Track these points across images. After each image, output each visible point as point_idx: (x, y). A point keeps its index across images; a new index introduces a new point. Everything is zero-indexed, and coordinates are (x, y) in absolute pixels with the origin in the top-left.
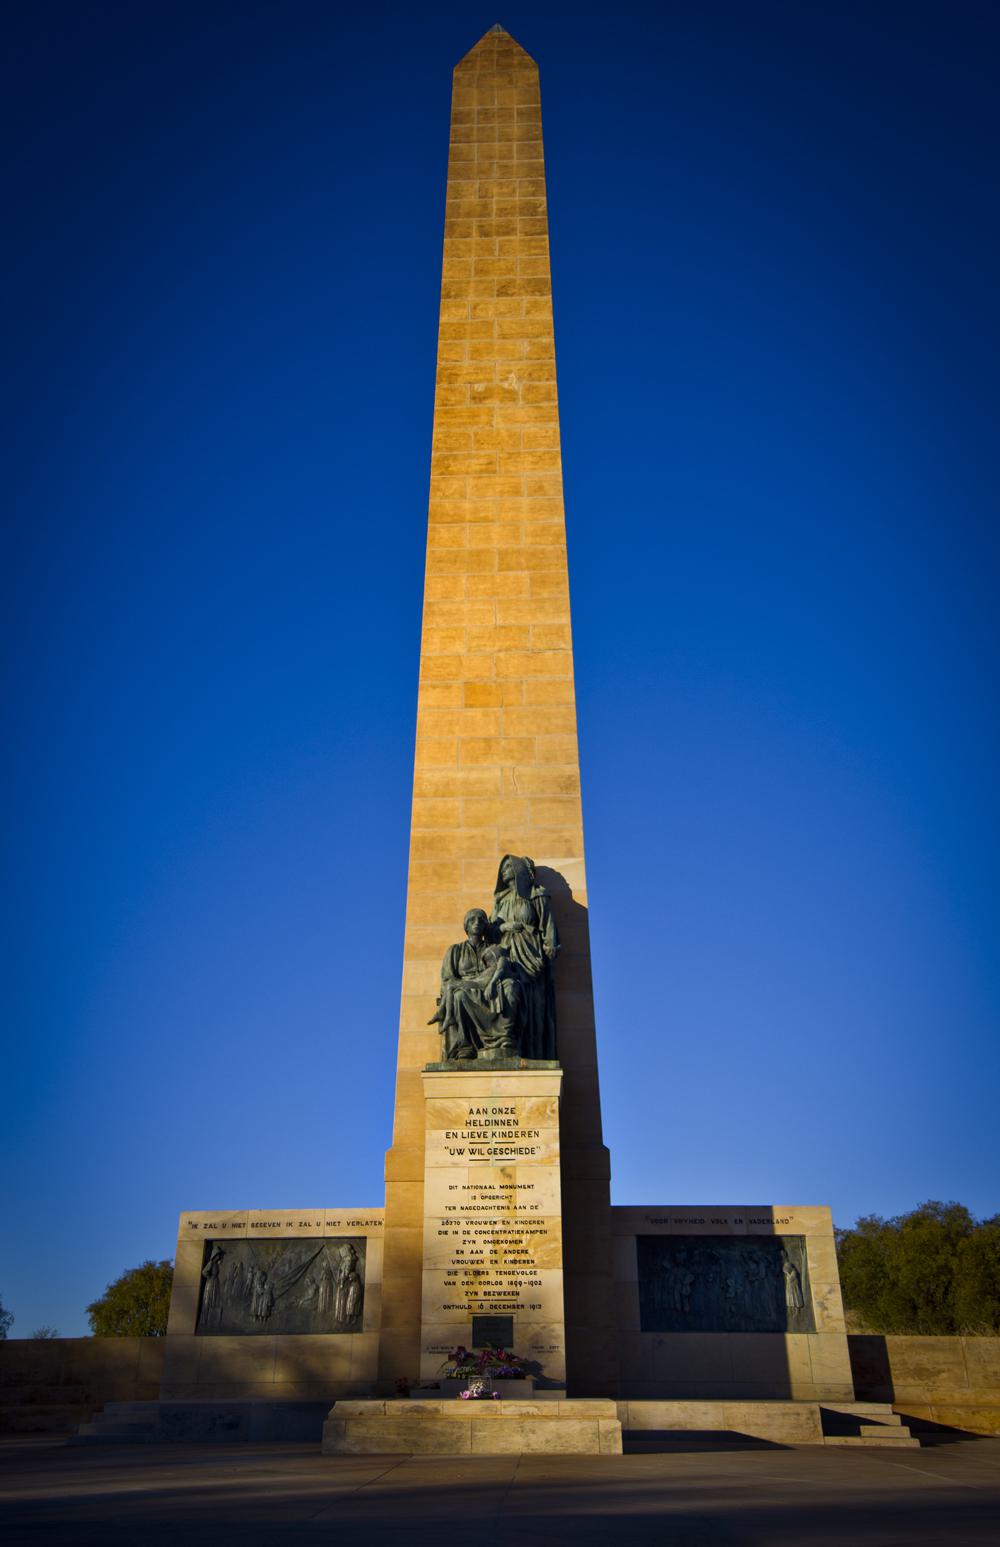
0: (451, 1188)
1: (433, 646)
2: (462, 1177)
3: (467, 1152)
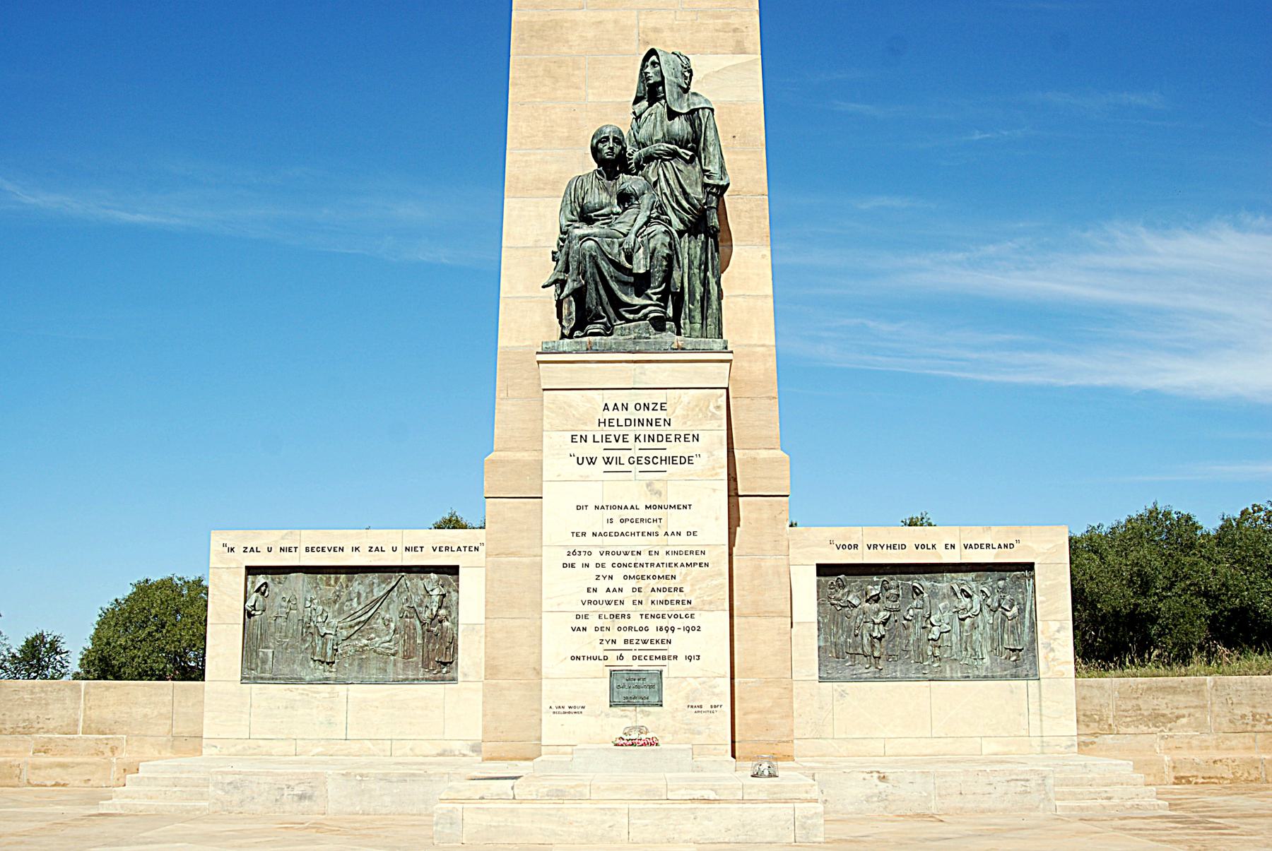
0: (579, 508)
3: (600, 462)
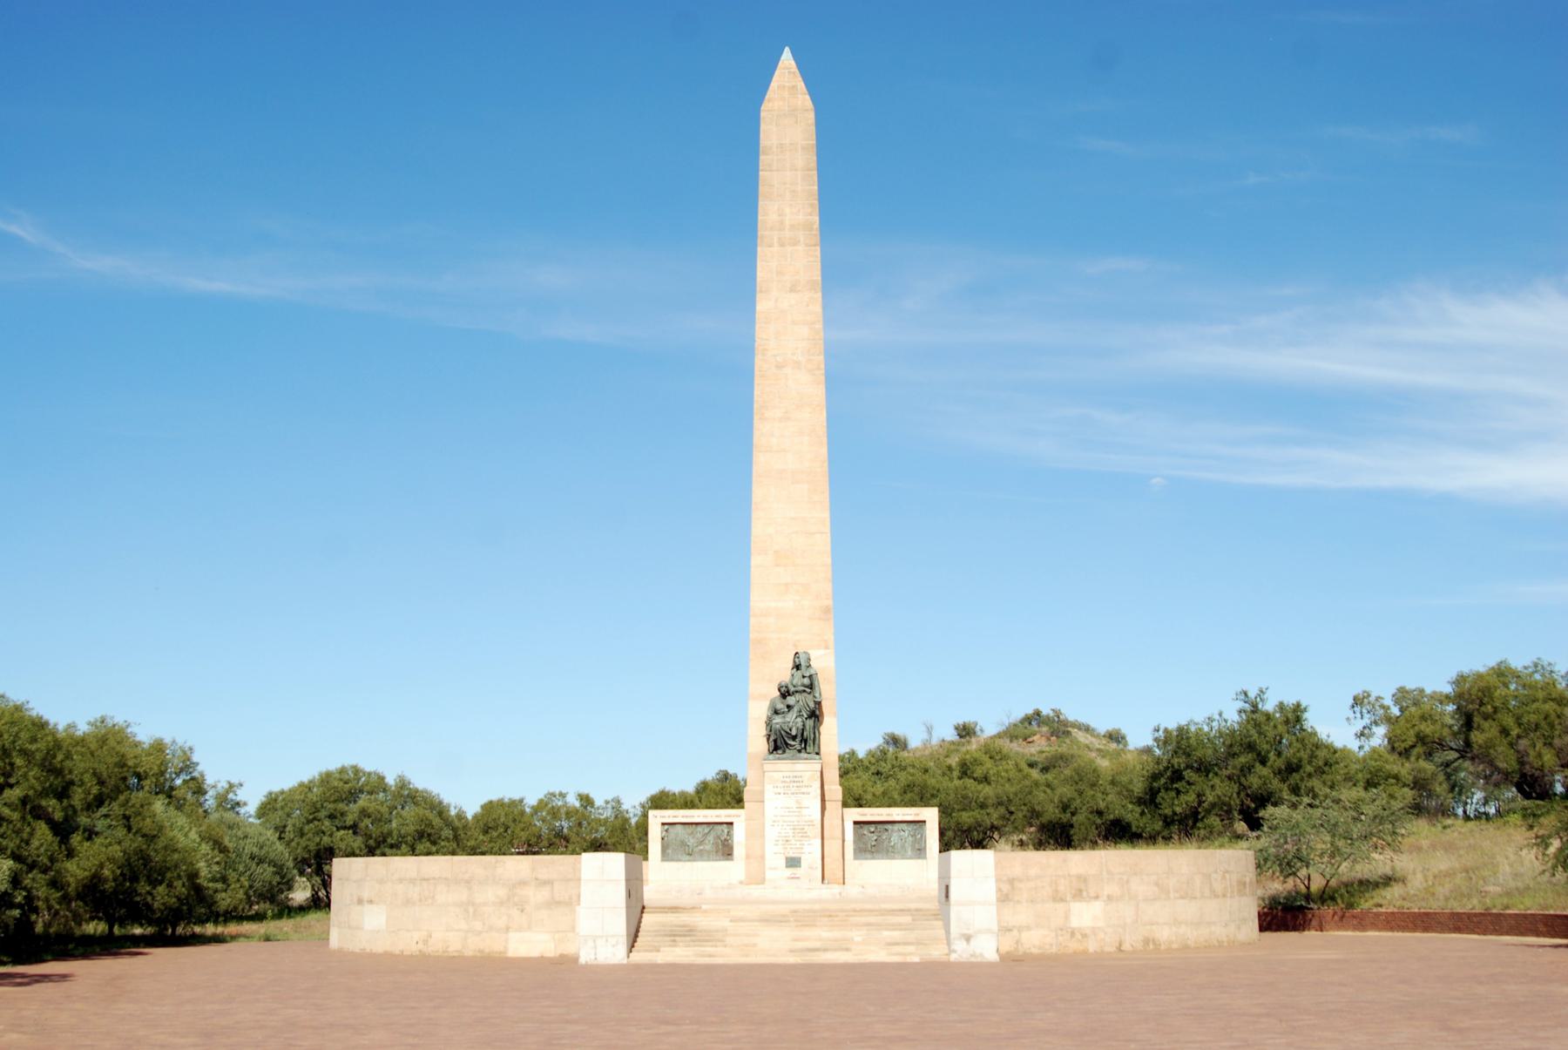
1: (759, 528)
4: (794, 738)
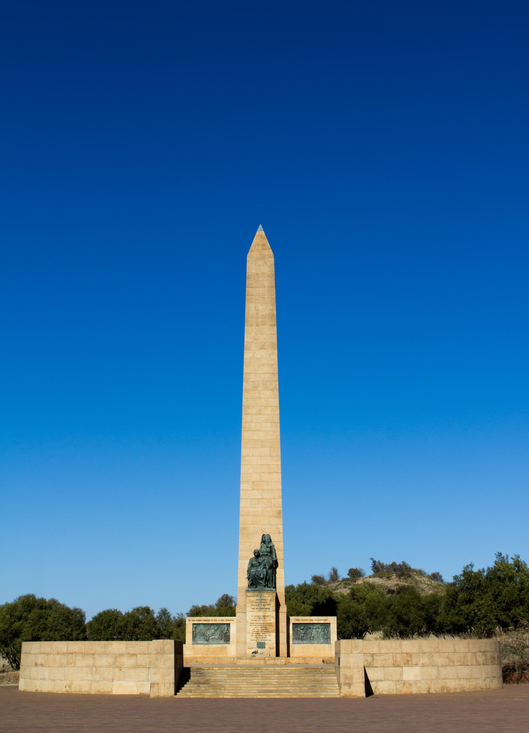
1: (244, 469)
2: (254, 614)
4: (262, 579)
